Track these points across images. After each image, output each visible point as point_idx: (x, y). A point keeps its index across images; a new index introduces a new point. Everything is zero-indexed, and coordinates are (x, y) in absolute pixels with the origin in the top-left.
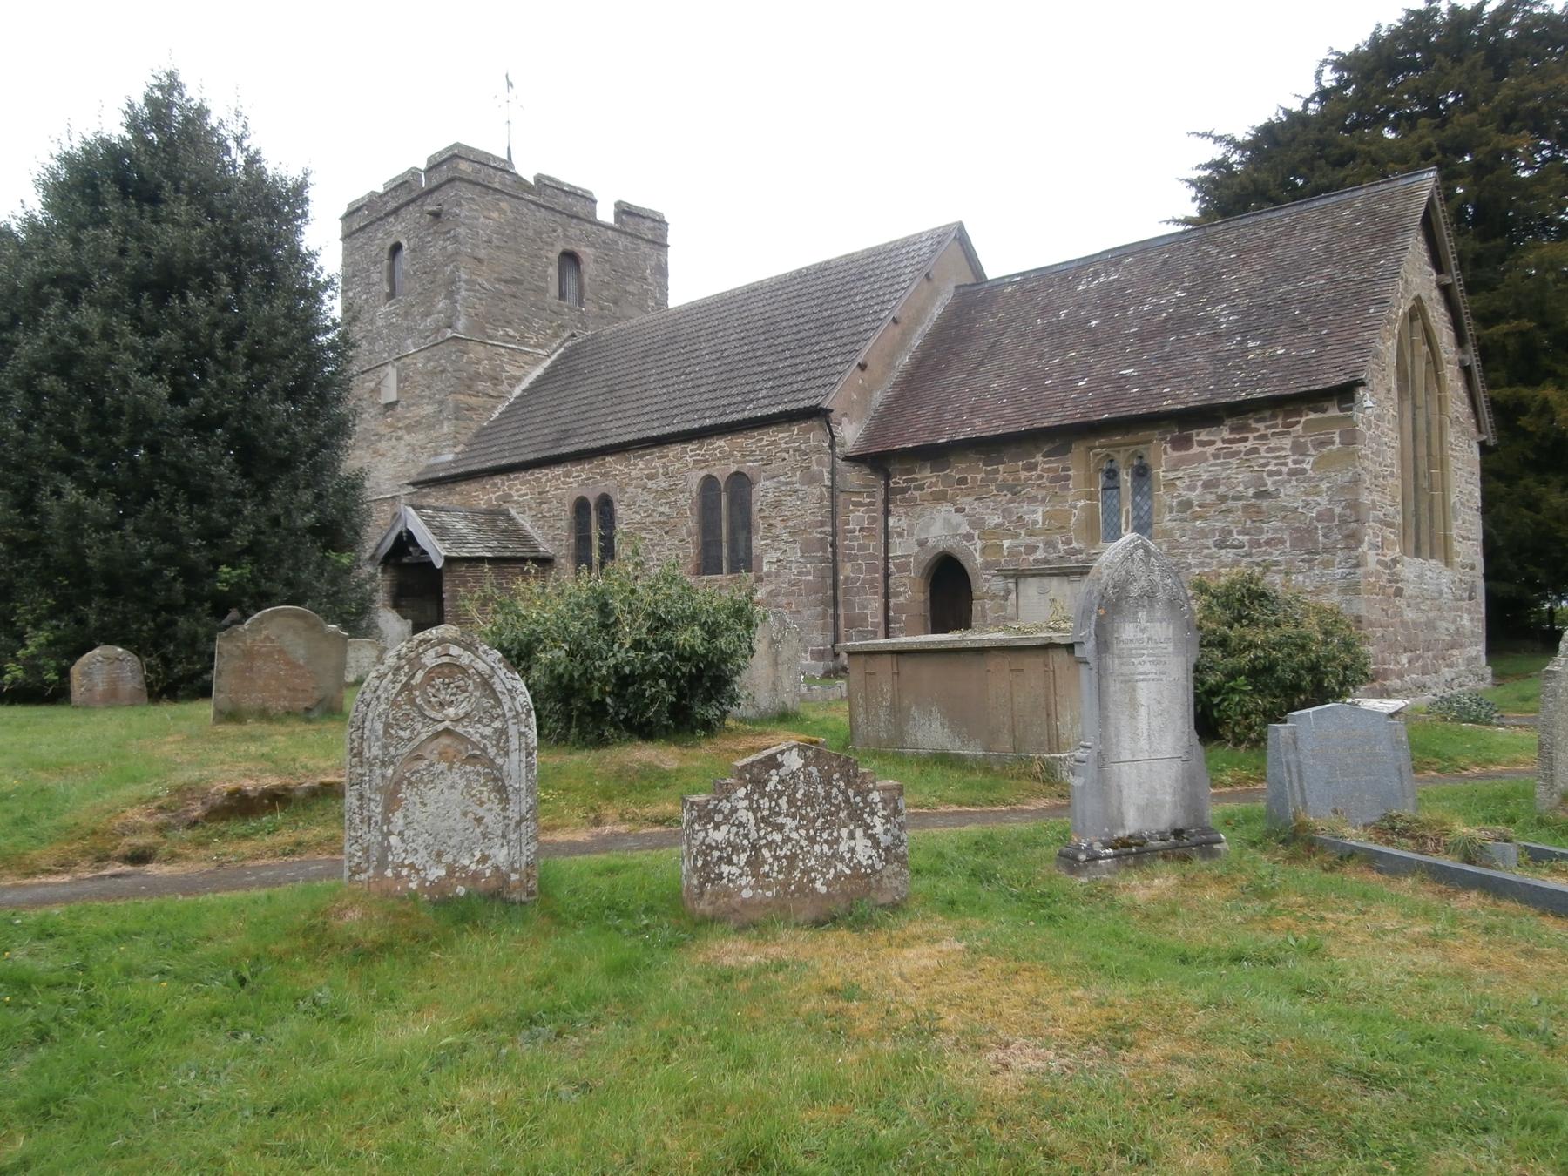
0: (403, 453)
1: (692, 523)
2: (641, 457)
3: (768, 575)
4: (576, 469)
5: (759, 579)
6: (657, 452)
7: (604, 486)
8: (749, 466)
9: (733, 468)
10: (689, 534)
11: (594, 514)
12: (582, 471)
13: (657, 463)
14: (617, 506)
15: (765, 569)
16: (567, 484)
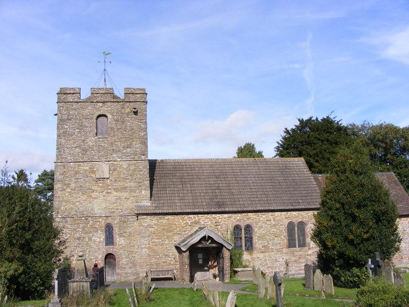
0: (114, 199)
1: (285, 234)
2: (264, 215)
3: (312, 248)
4: (234, 216)
5: (309, 249)
6: (270, 213)
7: (248, 222)
8: (304, 220)
9: (300, 220)
10: (285, 237)
11: (243, 230)
12: (239, 216)
13: (271, 217)
14: (254, 228)
15: (311, 246)
16: (236, 219)
